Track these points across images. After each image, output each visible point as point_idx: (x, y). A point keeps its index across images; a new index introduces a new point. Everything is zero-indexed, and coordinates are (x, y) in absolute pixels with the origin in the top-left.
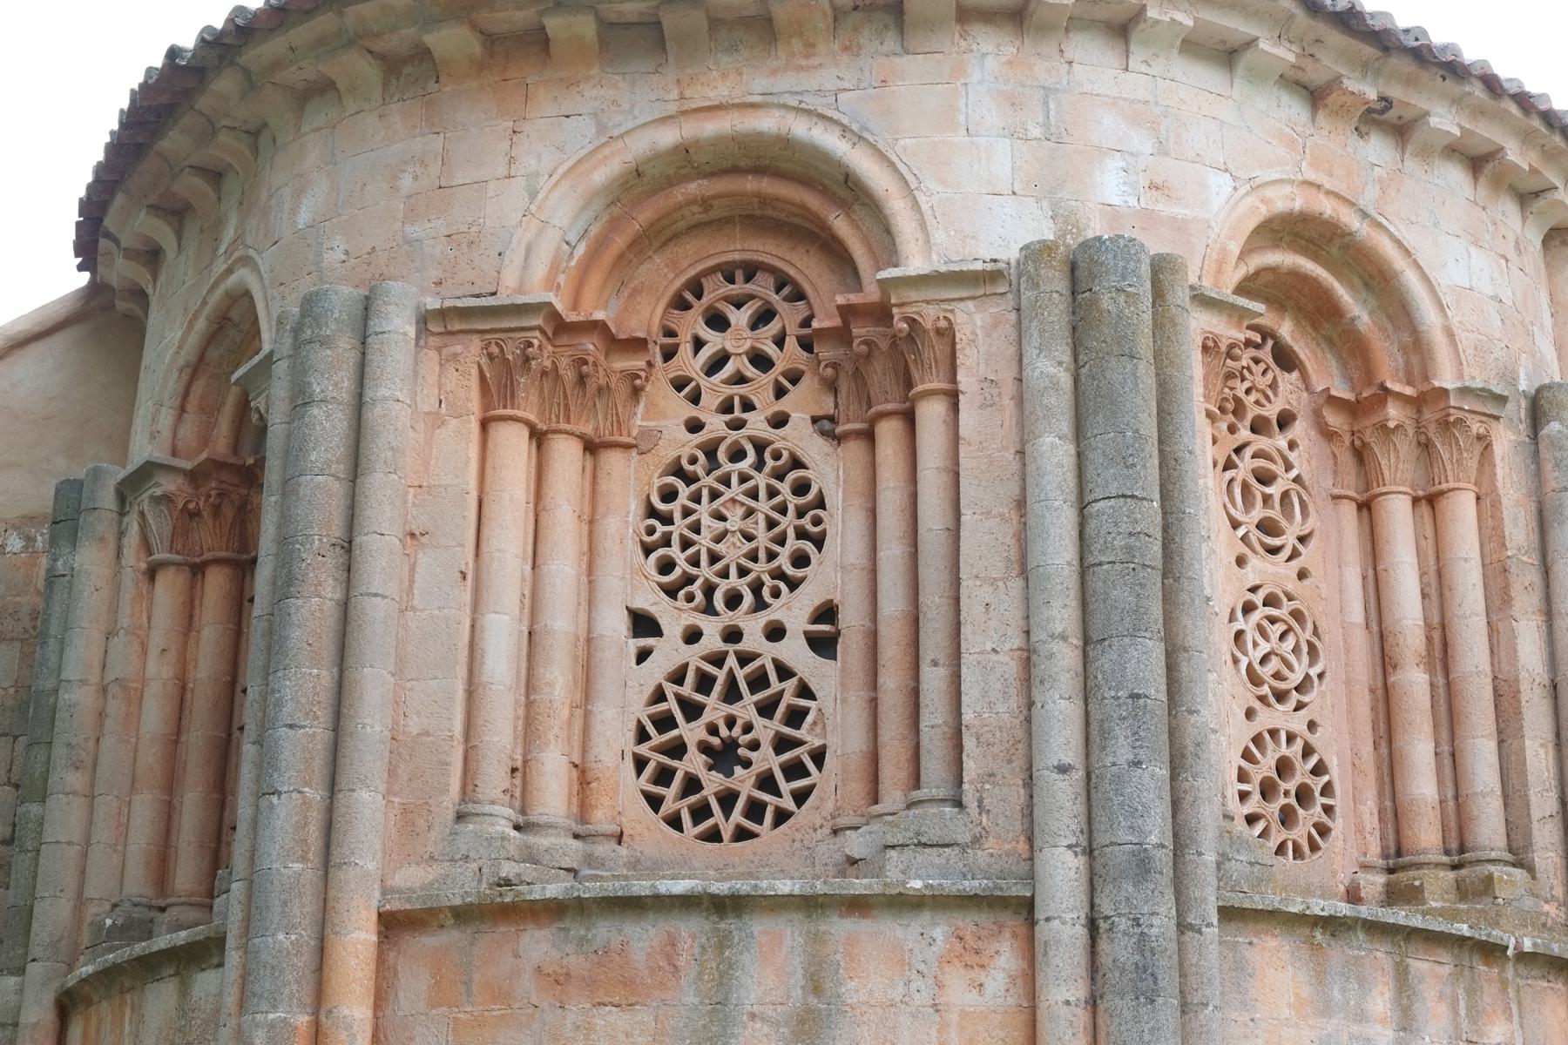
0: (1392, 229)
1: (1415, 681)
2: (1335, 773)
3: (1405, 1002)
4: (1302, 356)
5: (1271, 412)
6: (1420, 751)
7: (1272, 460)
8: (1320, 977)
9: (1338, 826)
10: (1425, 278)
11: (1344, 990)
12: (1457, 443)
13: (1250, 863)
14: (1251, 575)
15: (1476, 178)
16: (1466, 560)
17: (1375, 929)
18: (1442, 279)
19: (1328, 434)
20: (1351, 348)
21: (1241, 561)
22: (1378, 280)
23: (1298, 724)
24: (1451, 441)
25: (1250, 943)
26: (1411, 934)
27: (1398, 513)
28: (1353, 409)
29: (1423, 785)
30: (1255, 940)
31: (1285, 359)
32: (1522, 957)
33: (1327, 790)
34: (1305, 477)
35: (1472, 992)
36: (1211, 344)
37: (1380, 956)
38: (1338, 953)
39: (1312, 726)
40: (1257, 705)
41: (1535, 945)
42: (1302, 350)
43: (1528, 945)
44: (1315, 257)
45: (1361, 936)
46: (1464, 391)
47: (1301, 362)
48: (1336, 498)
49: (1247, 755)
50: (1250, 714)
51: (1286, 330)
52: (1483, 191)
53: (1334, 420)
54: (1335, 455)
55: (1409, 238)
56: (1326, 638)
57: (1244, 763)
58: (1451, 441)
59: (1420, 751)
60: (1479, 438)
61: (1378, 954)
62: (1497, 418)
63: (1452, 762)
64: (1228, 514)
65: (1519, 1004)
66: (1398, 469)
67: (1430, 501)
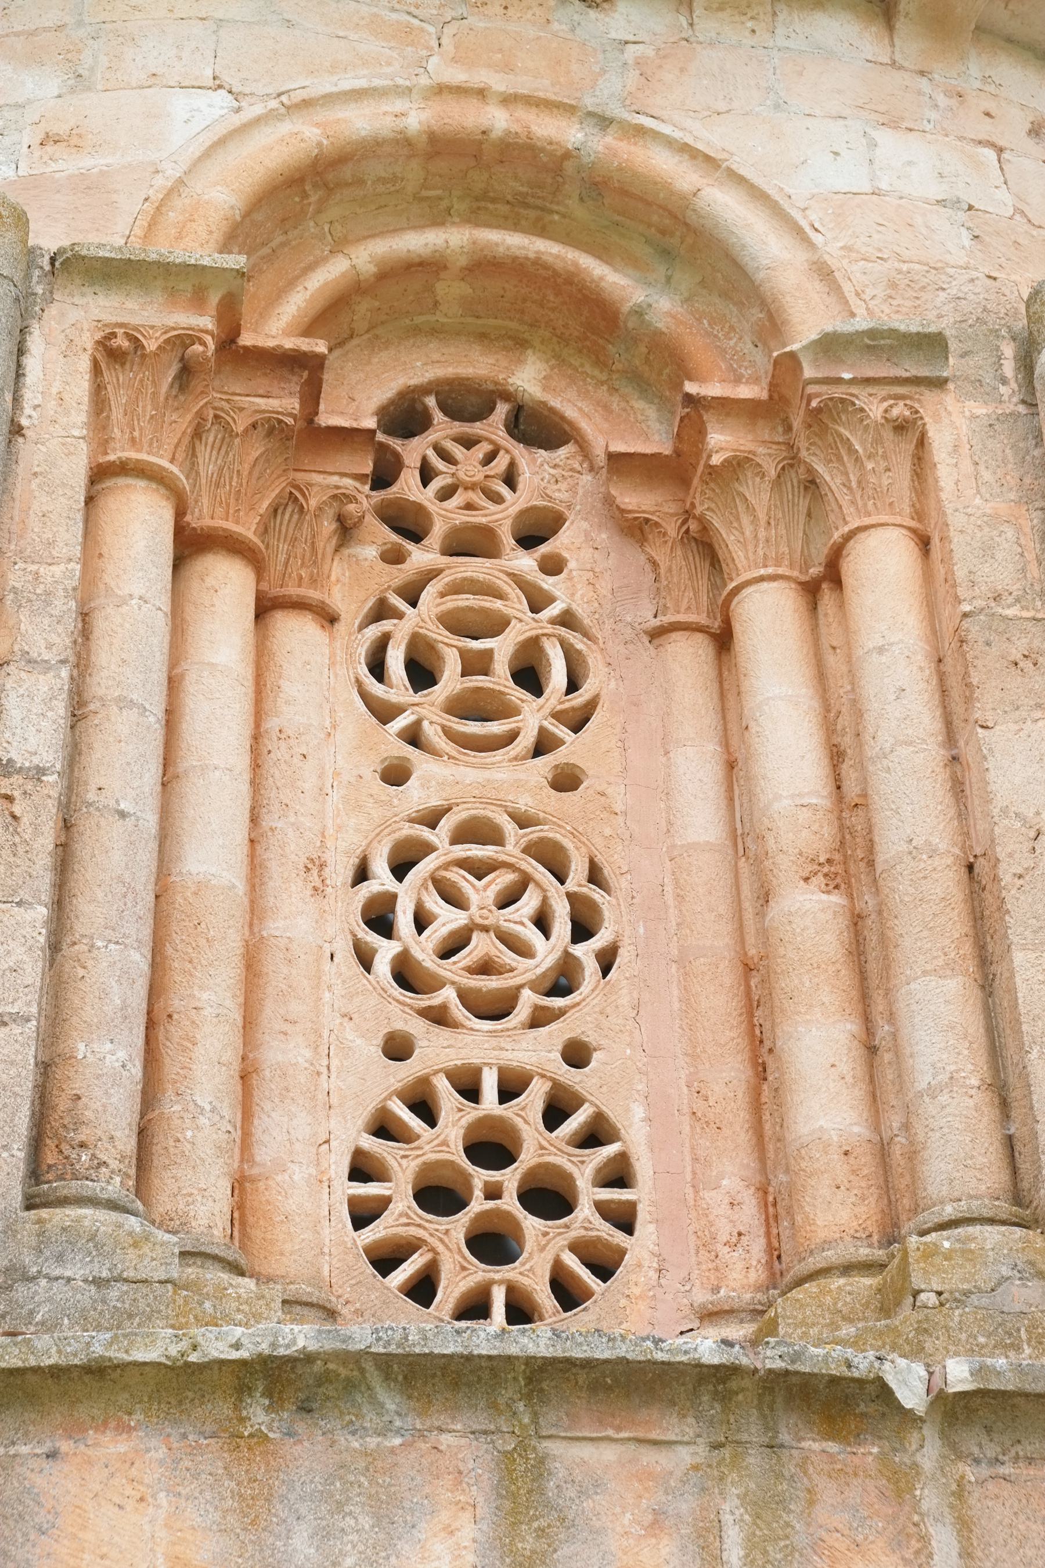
0: (666, 129)
1: (809, 914)
2: (636, 1136)
3: (528, 1544)
4: (570, 412)
5: (502, 517)
6: (818, 1044)
7: (500, 595)
8: (253, 1510)
9: (639, 1248)
10: (758, 195)
11: (324, 1535)
12: (851, 450)
13: (98, 1282)
14: (416, 795)
15: (890, 28)
16: (881, 650)
17: (423, 1378)
18: (796, 189)
19: (636, 529)
20: (653, 366)
21: (396, 775)
22: (676, 236)
23: (538, 1052)
24: (837, 451)
25: (52, 1455)
26: (544, 1377)
27: (768, 617)
28: (674, 470)
29: (825, 1107)
30: (65, 1446)
31: (537, 428)
32: (956, 1410)
33: (618, 1175)
34: (582, 611)
35: (764, 1507)
36: (121, 342)
37: (461, 1448)
38: (309, 1454)
39: (576, 1055)
40: (418, 1028)
41: (980, 1372)
42: (570, 406)
43: (959, 1374)
44: (541, 230)
45: (390, 1401)
46: (830, 345)
47: (577, 430)
48: (657, 634)
49: (384, 1128)
50: (397, 1049)
51: (528, 378)
52: (910, 44)
53: (635, 499)
54: (655, 564)
55: (709, 137)
56: (620, 883)
57: (371, 1144)
58: (837, 451)
59: (818, 1044)
60: (901, 427)
61: (446, 1440)
62: (939, 384)
63: (876, 1050)
64: (364, 695)
65: (964, 1525)
66: (755, 535)
67: (823, 582)
